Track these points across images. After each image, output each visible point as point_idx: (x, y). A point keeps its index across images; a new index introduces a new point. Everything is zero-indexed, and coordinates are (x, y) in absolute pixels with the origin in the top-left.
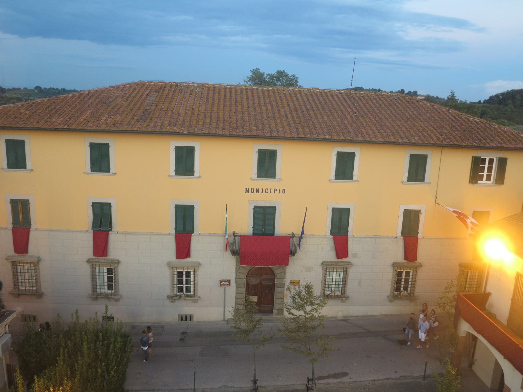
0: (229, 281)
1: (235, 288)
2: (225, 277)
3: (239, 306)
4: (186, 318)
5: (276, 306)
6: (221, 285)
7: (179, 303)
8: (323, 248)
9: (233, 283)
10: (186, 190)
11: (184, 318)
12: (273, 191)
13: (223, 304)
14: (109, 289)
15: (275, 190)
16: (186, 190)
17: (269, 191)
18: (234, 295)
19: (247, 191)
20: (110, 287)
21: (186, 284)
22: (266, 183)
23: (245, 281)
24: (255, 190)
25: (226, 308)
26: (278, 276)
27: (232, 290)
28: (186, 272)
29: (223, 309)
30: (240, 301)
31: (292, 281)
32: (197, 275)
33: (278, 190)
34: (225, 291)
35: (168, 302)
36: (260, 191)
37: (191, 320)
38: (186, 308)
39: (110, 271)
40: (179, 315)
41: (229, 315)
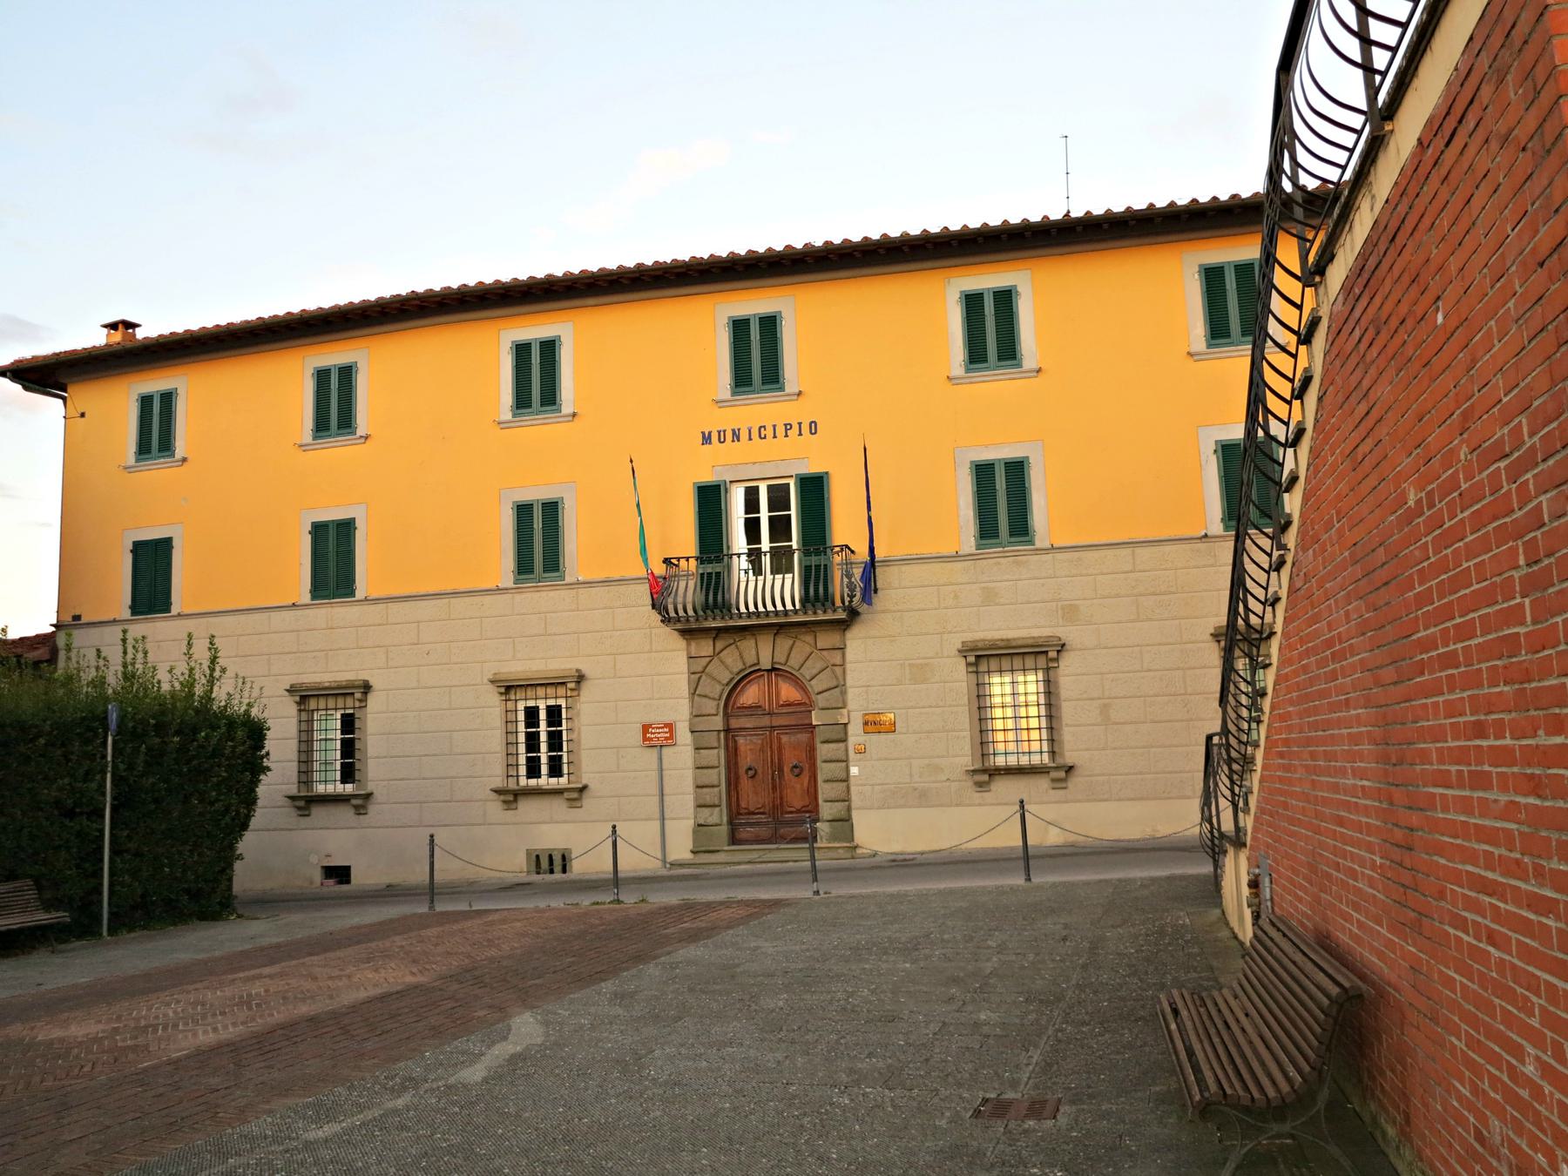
0: (670, 726)
2: (657, 717)
3: (706, 811)
4: (552, 863)
5: (826, 810)
6: (645, 739)
7: (527, 807)
8: (956, 597)
9: (684, 735)
10: (540, 459)
11: (545, 864)
12: (780, 431)
13: (657, 810)
14: (344, 781)
15: (788, 427)
16: (540, 459)
17: (769, 432)
19: (707, 439)
20: (348, 774)
21: (551, 748)
22: (760, 409)
23: (718, 722)
24: (729, 435)
26: (821, 700)
27: (682, 757)
28: (550, 709)
29: (657, 824)
30: (710, 795)
31: (870, 718)
32: (578, 714)
33: (796, 427)
34: (661, 759)
35: (495, 807)
36: (744, 435)
37: (564, 871)
38: (550, 827)
39: (348, 723)
40: (529, 852)
41: (681, 847)
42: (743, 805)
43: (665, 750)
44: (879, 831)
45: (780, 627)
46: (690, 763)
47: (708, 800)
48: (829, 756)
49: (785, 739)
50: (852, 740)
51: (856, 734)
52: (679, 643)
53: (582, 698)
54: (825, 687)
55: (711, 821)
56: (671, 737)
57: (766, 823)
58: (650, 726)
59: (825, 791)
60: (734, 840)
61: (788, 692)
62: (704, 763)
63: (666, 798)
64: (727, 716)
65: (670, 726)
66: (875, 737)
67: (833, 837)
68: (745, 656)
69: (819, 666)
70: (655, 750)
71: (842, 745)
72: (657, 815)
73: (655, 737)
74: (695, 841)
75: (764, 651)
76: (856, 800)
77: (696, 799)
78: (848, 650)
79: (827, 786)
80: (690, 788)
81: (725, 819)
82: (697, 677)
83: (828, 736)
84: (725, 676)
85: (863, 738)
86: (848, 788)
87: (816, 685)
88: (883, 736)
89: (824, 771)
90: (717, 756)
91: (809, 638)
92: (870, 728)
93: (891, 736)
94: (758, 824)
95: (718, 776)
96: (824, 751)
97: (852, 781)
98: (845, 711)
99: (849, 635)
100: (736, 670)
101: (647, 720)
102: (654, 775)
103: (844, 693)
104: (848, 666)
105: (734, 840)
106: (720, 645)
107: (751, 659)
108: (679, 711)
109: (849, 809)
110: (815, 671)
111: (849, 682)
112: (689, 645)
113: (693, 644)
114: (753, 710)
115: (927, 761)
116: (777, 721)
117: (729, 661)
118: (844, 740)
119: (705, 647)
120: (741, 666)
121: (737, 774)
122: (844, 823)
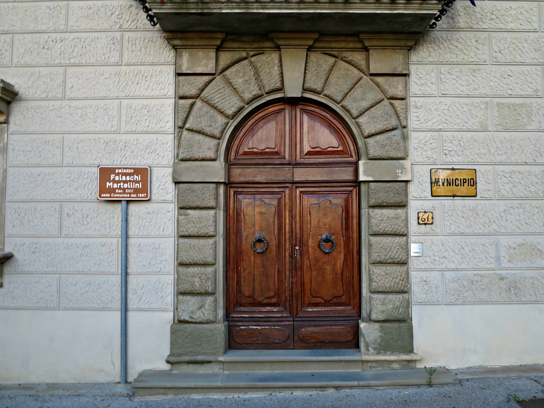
0: (143, 173)
1: (172, 208)
3: (193, 301)
5: (375, 305)
6: (103, 190)
9: (163, 186)
13: (118, 295)
18: (169, 245)
23: (217, 171)
25: (131, 315)
26: (374, 146)
27: (158, 220)
29: (117, 316)
30: (198, 278)
34: (126, 220)
41: (152, 351)
42: (246, 290)
43: (133, 207)
44: (450, 335)
46: (171, 229)
47: (197, 285)
48: (383, 227)
49: (309, 201)
50: (414, 206)
52: (169, 55)
53: (12, 127)
54: (380, 127)
55: (199, 316)
56: (144, 190)
57: (280, 320)
58: (112, 170)
59: (372, 276)
60: (233, 342)
61: (318, 135)
62: (193, 231)
63: (131, 279)
64: (229, 164)
65: (143, 173)
66: (448, 202)
67: (384, 346)
68: (264, 76)
69: (373, 96)
70: (118, 209)
71: (400, 211)
72: (118, 304)
73: (122, 188)
74: (171, 349)
75: (293, 71)
77: (178, 281)
78: (413, 78)
79: (378, 270)
80: (170, 265)
81: (221, 313)
82: (187, 102)
83: (382, 197)
84: (231, 104)
85: (430, 204)
86: (407, 273)
87: (368, 124)
88: (458, 202)
89: (373, 248)
90: (213, 221)
91: (358, 58)
92: (440, 190)
94: (267, 320)
95: (214, 249)
96: (376, 219)
97: (413, 264)
98: (407, 163)
99: (414, 57)
100: (248, 96)
101: (107, 163)
102: (116, 243)
103: (405, 138)
104: (412, 101)
105: (233, 342)
106: (226, 58)
108: (158, 152)
109: (408, 305)
110: (365, 104)
111: (413, 121)
112: (178, 56)
114: (267, 158)
115: (519, 240)
116: (300, 175)
117: (238, 82)
118: (403, 205)
119: (205, 61)
120: (255, 91)
121: (239, 253)
122: (399, 328)
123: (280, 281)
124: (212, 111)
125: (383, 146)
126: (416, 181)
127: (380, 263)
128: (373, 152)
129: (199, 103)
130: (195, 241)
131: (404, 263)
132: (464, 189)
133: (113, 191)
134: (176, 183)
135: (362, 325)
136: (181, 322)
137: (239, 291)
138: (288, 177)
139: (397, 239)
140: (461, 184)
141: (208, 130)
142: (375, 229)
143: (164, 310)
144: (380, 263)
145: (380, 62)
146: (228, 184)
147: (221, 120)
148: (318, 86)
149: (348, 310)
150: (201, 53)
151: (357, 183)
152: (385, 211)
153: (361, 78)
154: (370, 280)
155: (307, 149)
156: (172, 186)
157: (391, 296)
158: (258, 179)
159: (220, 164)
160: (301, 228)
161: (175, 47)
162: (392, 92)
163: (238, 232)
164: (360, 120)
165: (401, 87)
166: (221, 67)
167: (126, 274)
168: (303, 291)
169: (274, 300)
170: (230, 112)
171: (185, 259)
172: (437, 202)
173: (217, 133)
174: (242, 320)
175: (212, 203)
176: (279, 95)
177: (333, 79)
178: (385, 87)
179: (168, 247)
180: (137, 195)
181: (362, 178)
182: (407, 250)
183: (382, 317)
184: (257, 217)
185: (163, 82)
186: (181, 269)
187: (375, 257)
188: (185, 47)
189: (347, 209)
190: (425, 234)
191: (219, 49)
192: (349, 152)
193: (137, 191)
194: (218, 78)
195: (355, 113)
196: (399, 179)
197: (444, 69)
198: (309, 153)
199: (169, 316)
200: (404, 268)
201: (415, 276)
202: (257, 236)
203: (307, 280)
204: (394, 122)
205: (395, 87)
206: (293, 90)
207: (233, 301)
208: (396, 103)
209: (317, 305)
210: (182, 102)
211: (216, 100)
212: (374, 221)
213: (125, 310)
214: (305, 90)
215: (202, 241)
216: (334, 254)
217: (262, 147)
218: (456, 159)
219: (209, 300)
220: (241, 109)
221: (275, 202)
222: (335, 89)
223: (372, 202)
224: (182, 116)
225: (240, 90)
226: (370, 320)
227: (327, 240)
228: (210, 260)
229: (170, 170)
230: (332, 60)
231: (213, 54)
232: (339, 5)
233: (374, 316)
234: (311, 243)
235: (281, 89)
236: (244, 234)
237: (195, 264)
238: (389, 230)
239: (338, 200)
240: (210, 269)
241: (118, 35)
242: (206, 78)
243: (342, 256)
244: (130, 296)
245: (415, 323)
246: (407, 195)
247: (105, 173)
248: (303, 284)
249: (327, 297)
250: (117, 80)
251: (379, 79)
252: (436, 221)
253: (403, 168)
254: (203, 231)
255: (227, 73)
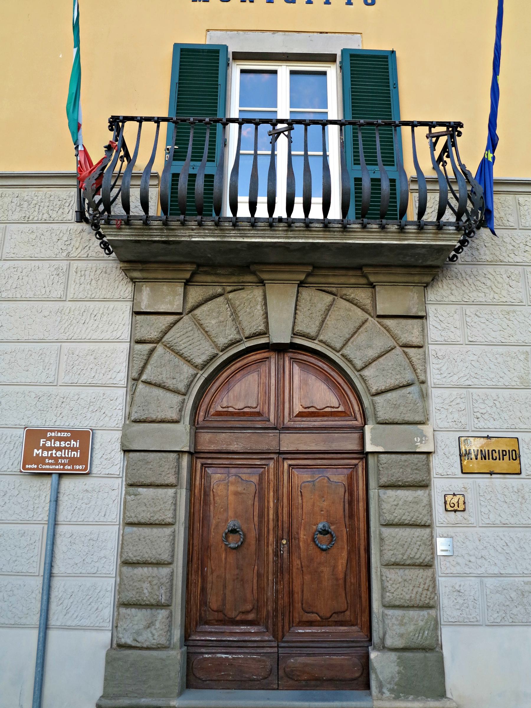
0: (84, 438)
1: (118, 485)
3: (139, 616)
5: (392, 626)
6: (28, 458)
9: (107, 456)
13: (36, 606)
18: (111, 535)
23: (180, 436)
25: (52, 634)
26: (384, 407)
27: (99, 502)
29: (33, 636)
34: (56, 501)
42: (214, 602)
43: (67, 484)
45: (313, 263)
46: (115, 514)
47: (147, 593)
48: (398, 515)
49: (301, 477)
50: (439, 487)
51: (444, 471)
52: (125, 289)
55: (147, 638)
57: (260, 645)
58: (42, 433)
59: (387, 584)
60: (194, 678)
61: (312, 391)
62: (144, 517)
63: (57, 583)
64: (196, 427)
65: (84, 438)
66: (484, 481)
67: (405, 689)
68: (243, 316)
69: (381, 342)
70: (47, 484)
71: (420, 493)
72: (35, 619)
73: (54, 458)
74: (105, 688)
75: (278, 310)
76: (448, 607)
77: (120, 587)
78: (431, 321)
79: (393, 575)
80: (110, 564)
81: (177, 634)
84: (201, 351)
85: (460, 483)
86: (434, 580)
87: (376, 378)
88: (498, 481)
89: (387, 544)
90: (170, 503)
91: (362, 295)
93: (512, 482)
94: (241, 645)
95: (170, 543)
96: (388, 503)
98: (427, 429)
99: (432, 295)
100: (222, 341)
101: (36, 423)
102: (40, 531)
103: (424, 396)
104: (432, 349)
105: (194, 678)
106: (196, 294)
107: (252, 323)
110: (371, 353)
111: (434, 375)
112: (136, 291)
113: (146, 291)
116: (289, 442)
117: (211, 323)
118: (424, 485)
119: (169, 297)
120: (233, 335)
121: (206, 548)
123: (261, 589)
124: (177, 360)
125: (396, 407)
126: (440, 452)
127: (396, 564)
128: (382, 415)
129: (160, 349)
130: (146, 531)
131: (428, 565)
132: (505, 464)
133: (41, 460)
134: (125, 451)
135: (373, 655)
136: (122, 646)
137: (204, 603)
138: (274, 447)
139: (418, 532)
140: (498, 458)
141: (170, 383)
142: (388, 517)
143: (99, 629)
144: (396, 564)
145: (389, 301)
146: (194, 454)
147: (187, 371)
148: (312, 331)
149: (354, 632)
150: (165, 288)
151: (363, 455)
152: (401, 493)
153: (366, 321)
154: (383, 589)
155: (298, 408)
156: (119, 455)
157: (412, 613)
158: (234, 447)
159: (184, 428)
160: (290, 515)
161: (133, 280)
162: (405, 338)
163: (205, 519)
164: (366, 373)
165: (416, 332)
166: (189, 305)
167: (50, 576)
168: (291, 603)
169: (251, 616)
170: (199, 361)
171: (132, 556)
172: (469, 481)
173: (181, 387)
174: (207, 644)
175: (172, 480)
176: (263, 340)
177: (330, 321)
178: (397, 331)
179: (109, 538)
180: (73, 467)
181: (369, 447)
182: (432, 547)
183: (400, 643)
184: (231, 498)
185: (117, 320)
186: (125, 569)
187: (389, 556)
188: (146, 280)
189: (350, 489)
190: (455, 525)
191: (187, 283)
192: (353, 413)
193: (73, 461)
194: (186, 318)
195: (359, 364)
196: (418, 450)
197: (470, 310)
198: (301, 415)
199: (105, 637)
200: (428, 572)
201: (444, 584)
202: (231, 524)
203: (297, 588)
204: (409, 376)
205: (409, 332)
206: (280, 335)
207: (196, 616)
208: (411, 352)
209: (310, 623)
210: (139, 347)
211: (182, 346)
212: (386, 507)
213: (45, 627)
214: (295, 334)
215: (156, 531)
216: (334, 551)
217: (240, 405)
218: (491, 424)
219: (162, 614)
220: (213, 357)
221: (255, 479)
222: (334, 334)
223: (384, 480)
224: (138, 364)
225: (213, 333)
226: (383, 648)
227: (324, 532)
228: (165, 557)
229: (118, 435)
230: (329, 298)
231: (180, 289)
232: (336, 234)
233: (389, 642)
234: (303, 535)
235: (264, 333)
236: (214, 522)
237: (146, 563)
238: (407, 518)
239: (339, 477)
240: (165, 571)
241: (64, 264)
242: (171, 319)
243: (345, 554)
244: (53, 606)
245: (446, 652)
246: (429, 471)
247: (34, 436)
248: (291, 593)
249: (325, 612)
250: (59, 319)
251: (389, 322)
252: (469, 506)
253: (423, 435)
254: (158, 517)
255: (197, 312)
